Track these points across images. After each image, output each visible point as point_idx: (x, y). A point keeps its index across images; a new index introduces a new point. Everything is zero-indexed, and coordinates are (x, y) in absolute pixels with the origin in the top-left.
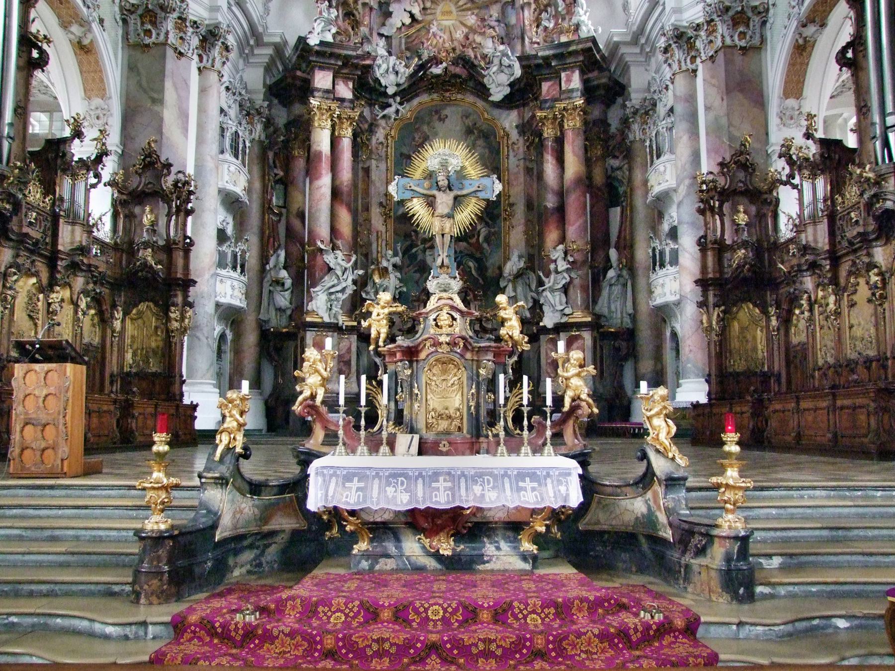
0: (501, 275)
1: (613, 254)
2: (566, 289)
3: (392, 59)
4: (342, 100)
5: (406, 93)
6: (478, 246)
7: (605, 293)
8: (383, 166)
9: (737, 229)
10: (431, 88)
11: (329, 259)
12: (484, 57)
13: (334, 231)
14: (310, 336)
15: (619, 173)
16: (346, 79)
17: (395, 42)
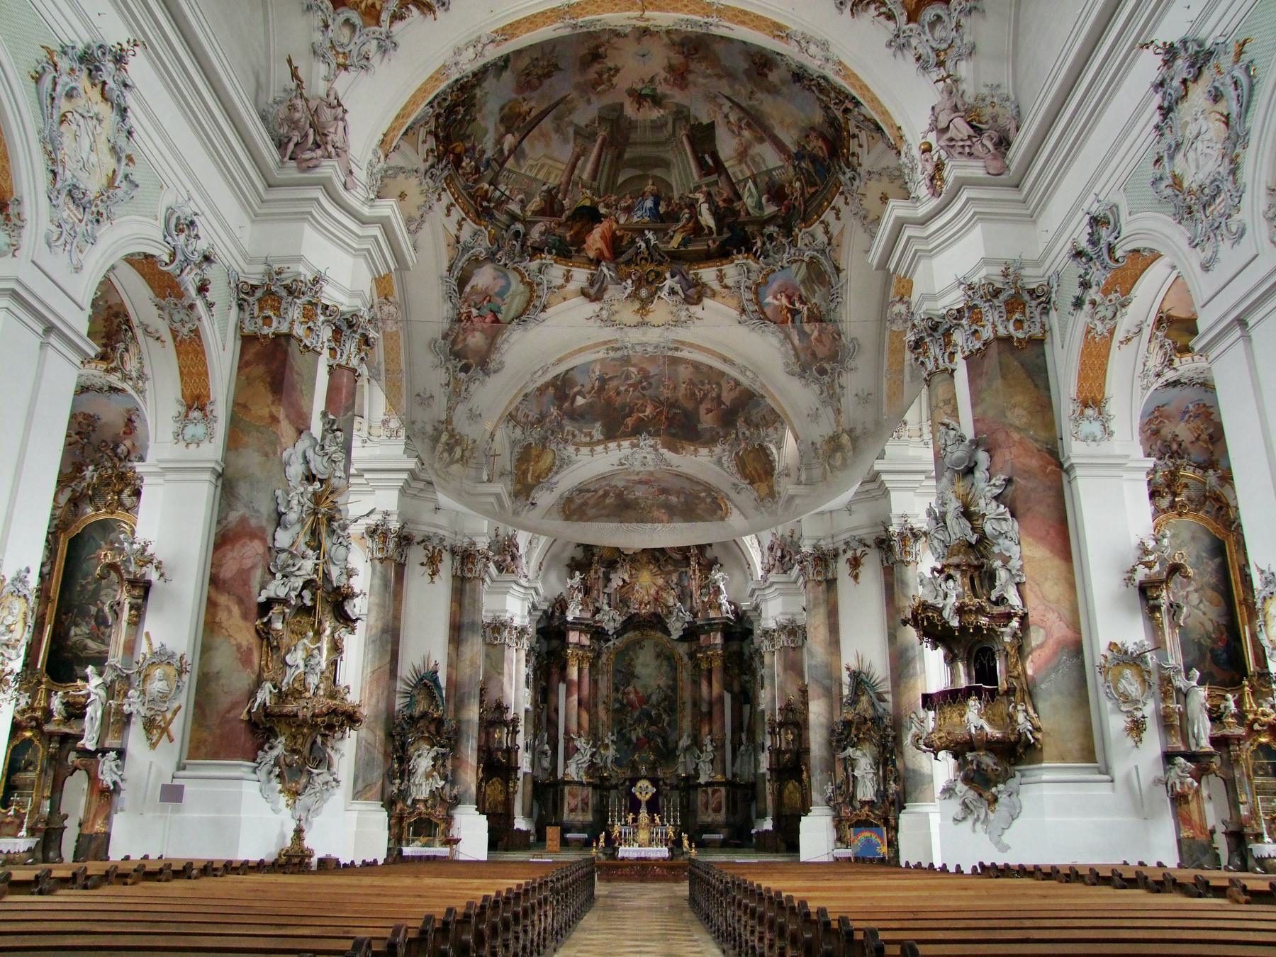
0: (677, 747)
1: (744, 736)
2: (712, 761)
3: (612, 613)
4: (583, 646)
5: (619, 633)
6: (663, 728)
7: (739, 760)
8: (605, 678)
9: (788, 743)
10: (634, 629)
11: (578, 744)
12: (668, 607)
13: (579, 725)
14: (567, 789)
15: (748, 685)
16: (586, 633)
17: (613, 598)
